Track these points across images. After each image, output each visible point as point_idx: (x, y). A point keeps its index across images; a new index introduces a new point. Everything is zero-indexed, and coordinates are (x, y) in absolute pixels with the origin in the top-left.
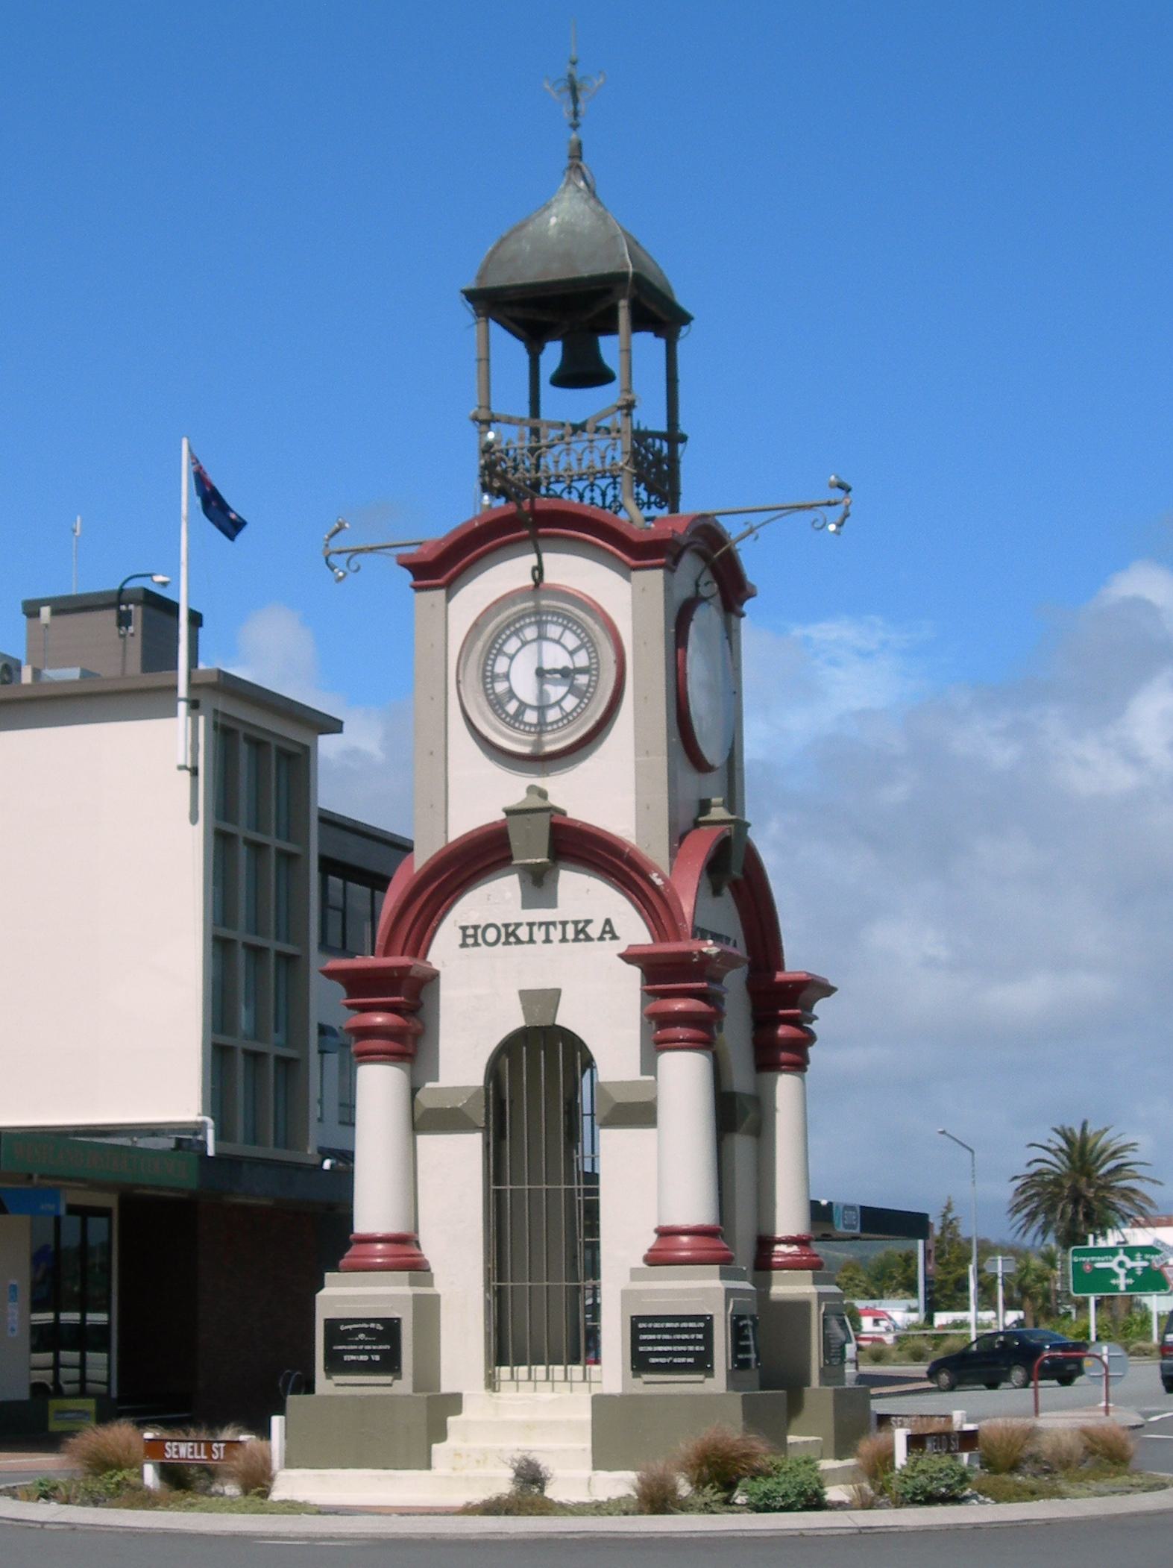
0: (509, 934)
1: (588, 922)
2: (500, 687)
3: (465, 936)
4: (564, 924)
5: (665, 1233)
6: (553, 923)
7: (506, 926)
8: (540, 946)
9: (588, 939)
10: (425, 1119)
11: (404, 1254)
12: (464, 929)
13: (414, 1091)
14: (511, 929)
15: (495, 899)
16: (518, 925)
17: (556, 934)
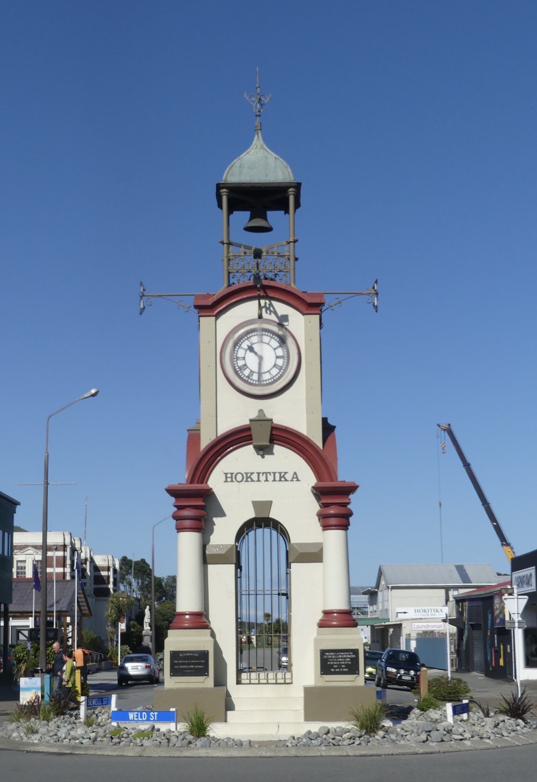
0: (248, 477)
1: (286, 473)
3: (226, 478)
4: (274, 473)
5: (326, 613)
6: (270, 473)
7: (247, 474)
8: (263, 483)
9: (286, 480)
12: (226, 474)
13: (204, 547)
14: (249, 475)
16: (252, 473)
17: (271, 478)
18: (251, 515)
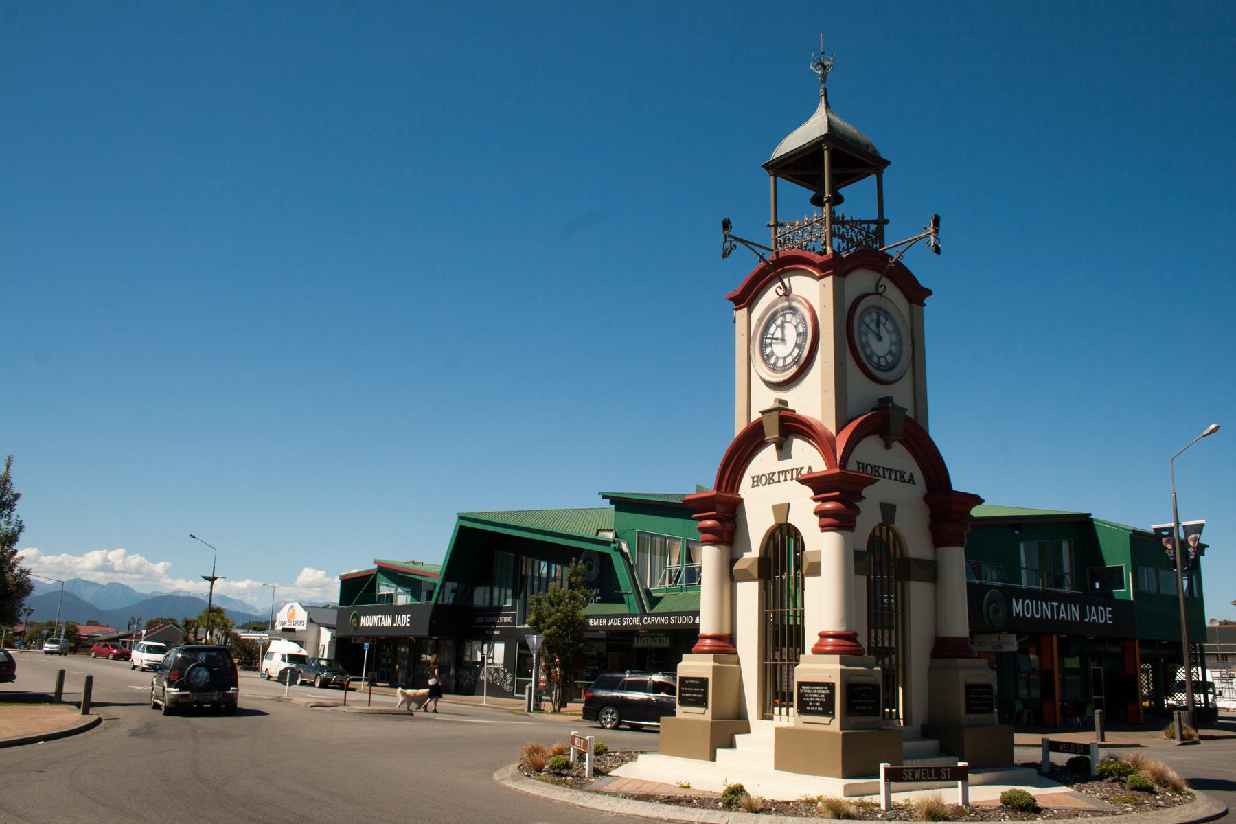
0: (770, 479)
2: (768, 350)
10: (731, 576)
15: (765, 460)
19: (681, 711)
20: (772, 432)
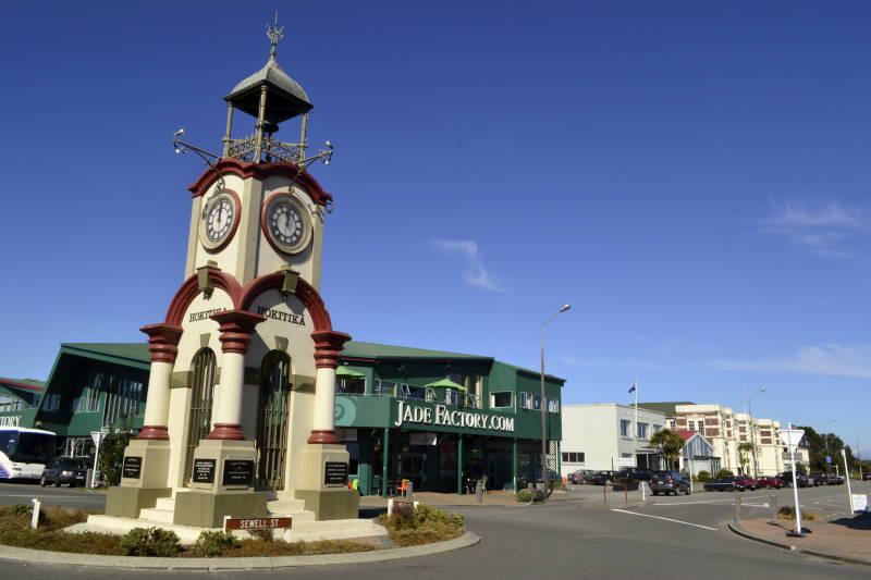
2: (210, 227)
11: (161, 433)
15: (199, 304)
18: (198, 347)
19: (125, 482)
20: (203, 282)
